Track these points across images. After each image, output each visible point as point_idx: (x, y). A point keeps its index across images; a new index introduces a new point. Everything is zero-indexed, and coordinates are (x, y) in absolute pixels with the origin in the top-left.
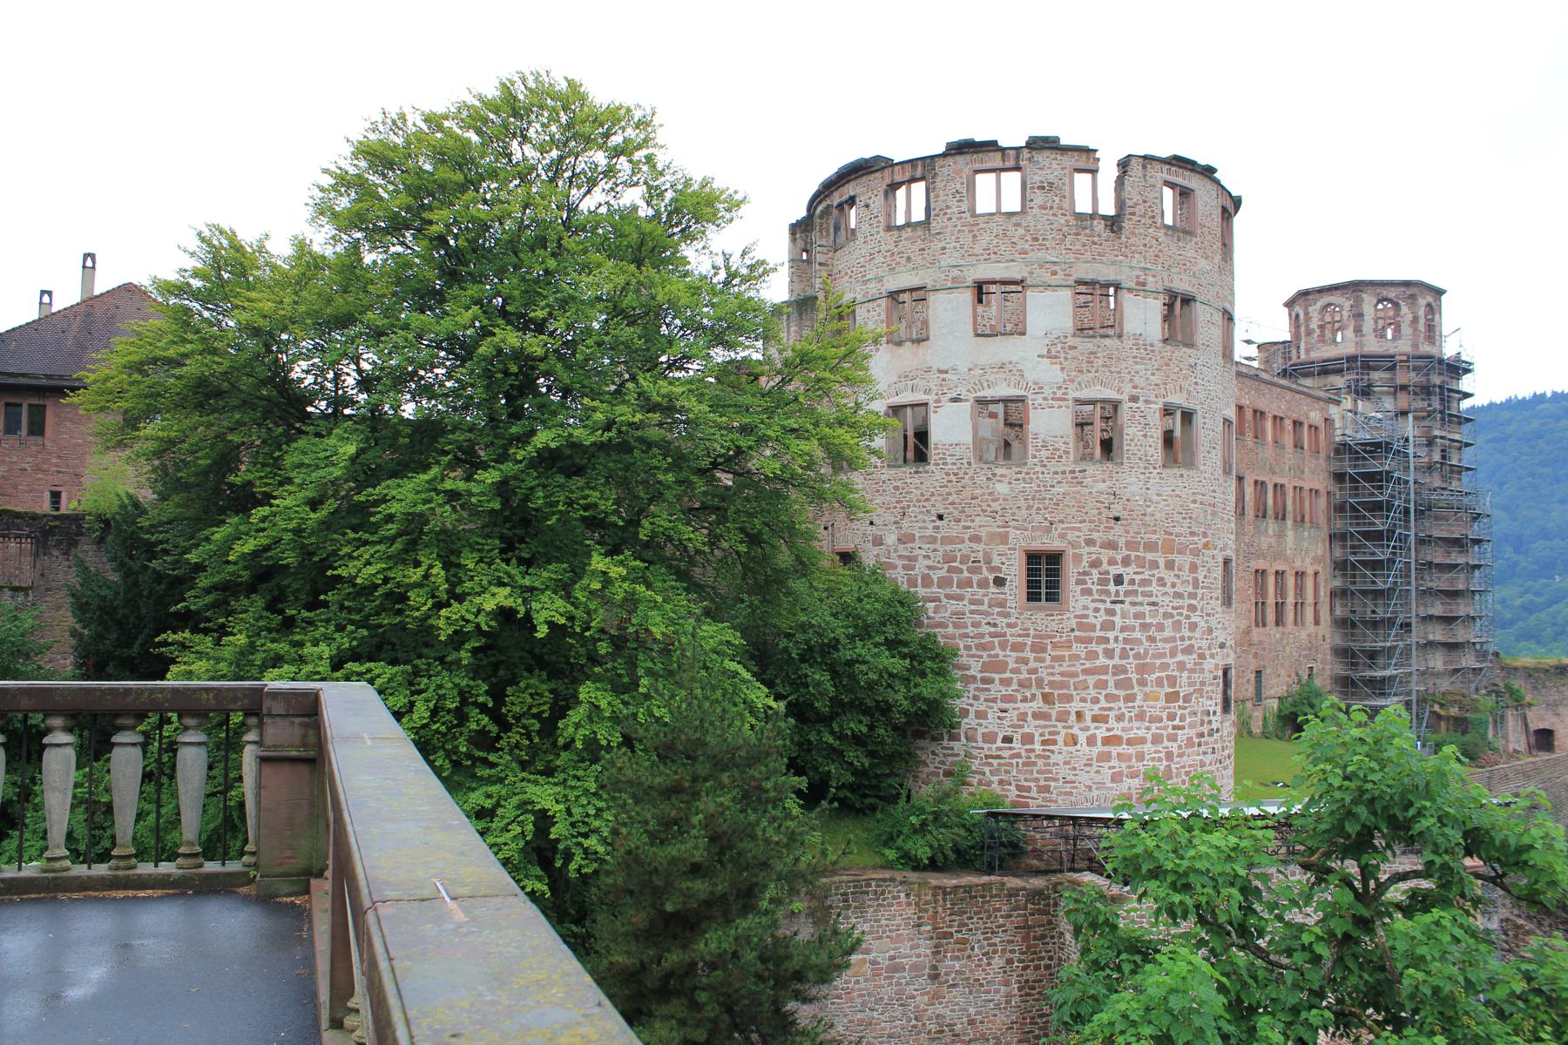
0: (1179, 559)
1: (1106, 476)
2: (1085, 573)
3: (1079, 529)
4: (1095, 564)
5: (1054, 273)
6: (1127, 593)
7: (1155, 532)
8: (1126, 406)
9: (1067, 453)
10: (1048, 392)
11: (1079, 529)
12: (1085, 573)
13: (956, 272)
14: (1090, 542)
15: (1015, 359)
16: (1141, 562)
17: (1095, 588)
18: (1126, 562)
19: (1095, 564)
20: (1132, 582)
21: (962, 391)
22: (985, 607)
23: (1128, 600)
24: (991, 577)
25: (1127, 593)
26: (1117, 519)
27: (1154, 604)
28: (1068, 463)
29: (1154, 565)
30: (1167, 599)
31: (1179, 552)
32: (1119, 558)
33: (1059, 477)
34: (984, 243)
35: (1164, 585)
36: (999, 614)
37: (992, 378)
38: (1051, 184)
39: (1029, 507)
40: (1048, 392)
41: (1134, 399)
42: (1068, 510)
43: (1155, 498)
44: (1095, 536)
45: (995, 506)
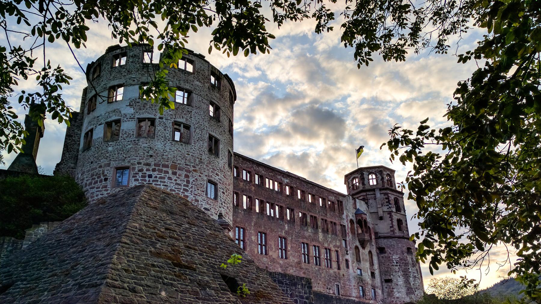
0: (179, 172)
1: (147, 142)
2: (136, 174)
3: (135, 159)
4: (140, 171)
5: (134, 81)
6: (153, 181)
7: (168, 162)
8: (157, 121)
9: (133, 135)
10: (128, 116)
11: (135, 159)
12: (136, 174)
13: (105, 86)
14: (139, 163)
15: (118, 108)
16: (160, 171)
17: (140, 179)
18: (154, 170)
19: (140, 171)
20: (156, 177)
21: (102, 121)
22: (100, 189)
23: (154, 183)
24: (103, 178)
25: (153, 181)
26: (151, 156)
27: (166, 186)
28: (133, 138)
29: (168, 172)
30: (172, 185)
31: (179, 169)
32: (151, 169)
33: (129, 143)
34: (113, 75)
35: (171, 180)
36: (105, 190)
37: (111, 115)
38: (135, 55)
39: (119, 153)
40: (128, 116)
41: (161, 118)
42: (132, 153)
43: (168, 150)
44: (141, 161)
45: (108, 155)
